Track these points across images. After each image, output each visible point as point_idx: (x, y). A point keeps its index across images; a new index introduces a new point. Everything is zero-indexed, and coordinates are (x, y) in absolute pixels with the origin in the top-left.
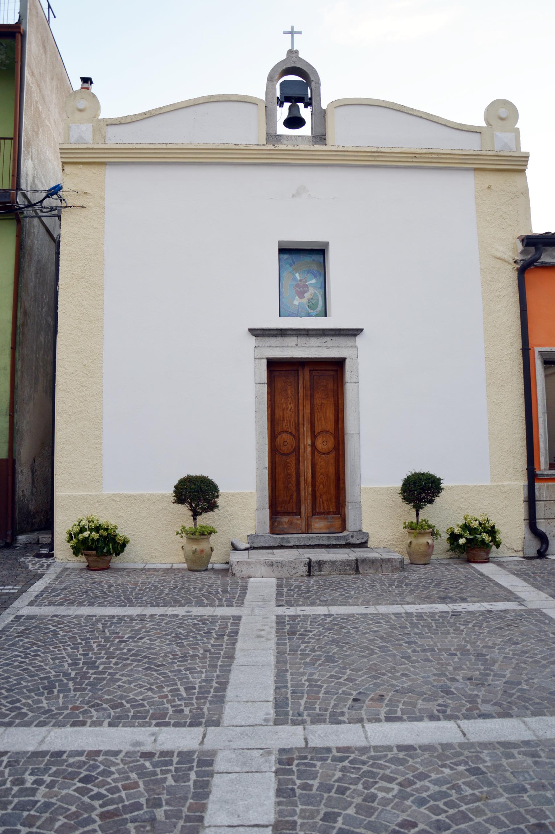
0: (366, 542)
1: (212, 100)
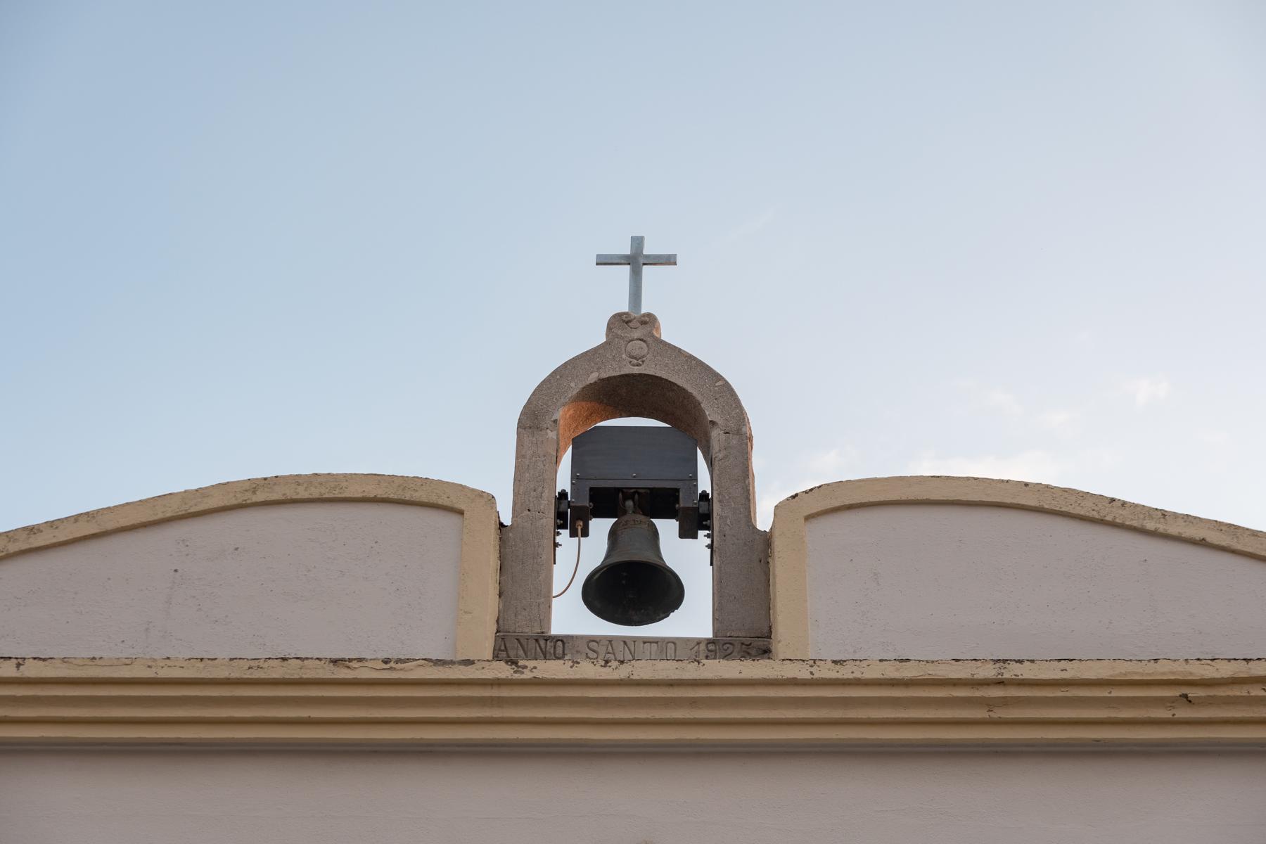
1: (260, 497)
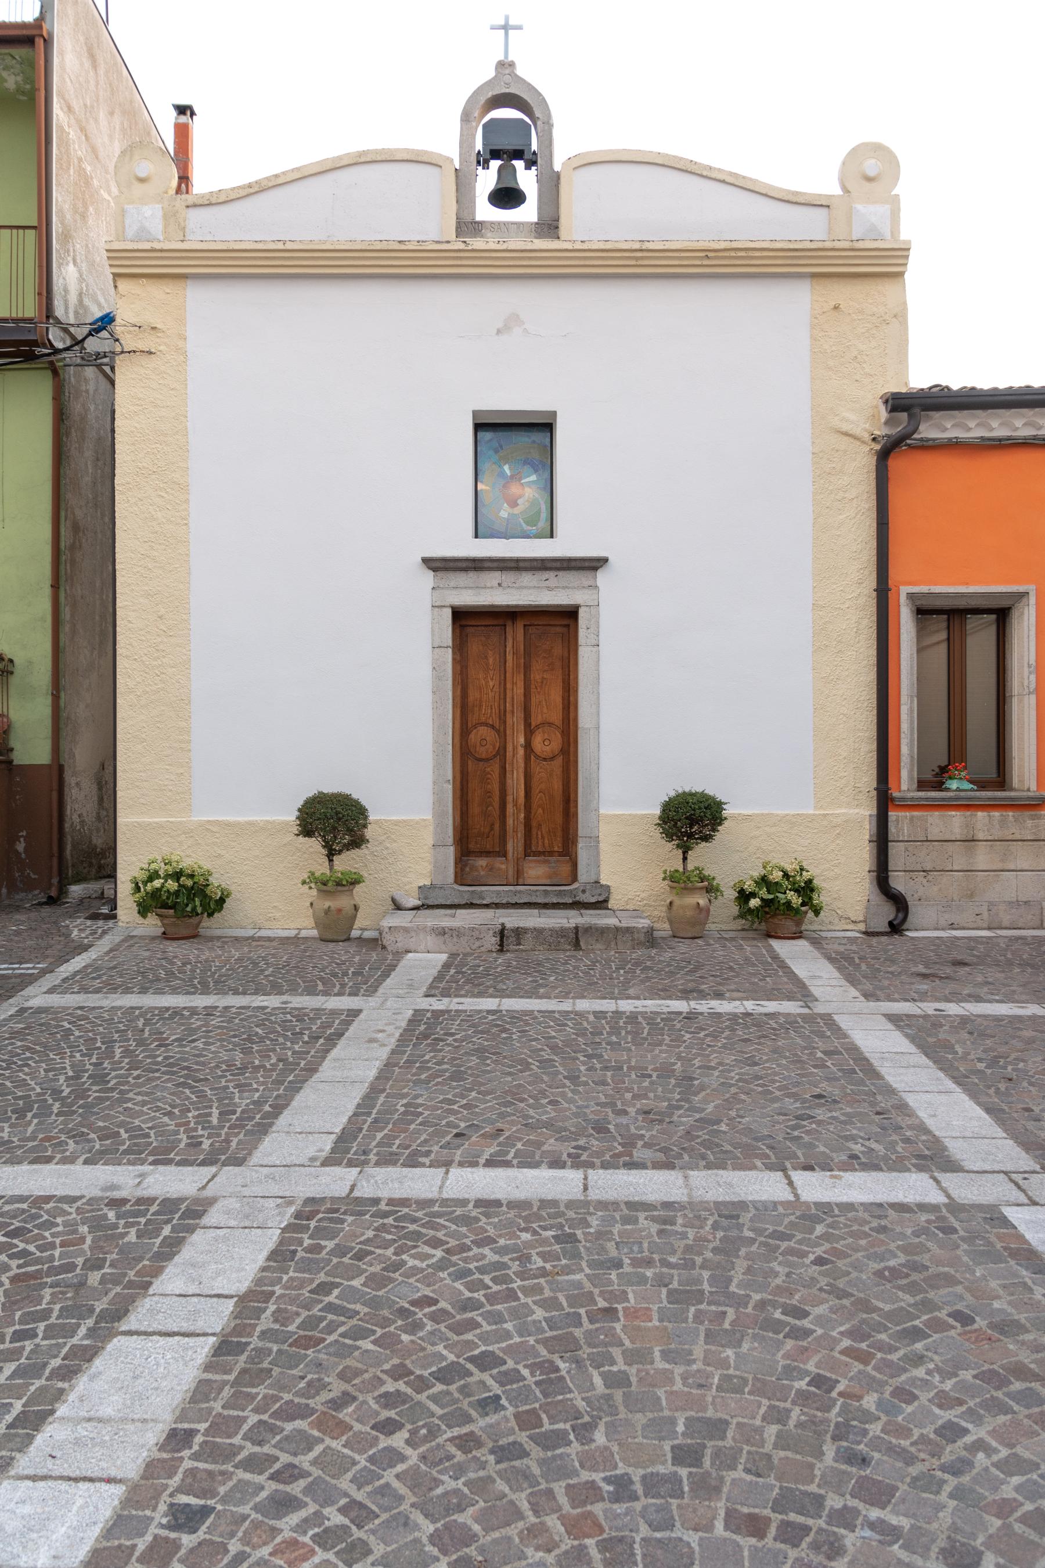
0: (606, 901)
1: (363, 160)
